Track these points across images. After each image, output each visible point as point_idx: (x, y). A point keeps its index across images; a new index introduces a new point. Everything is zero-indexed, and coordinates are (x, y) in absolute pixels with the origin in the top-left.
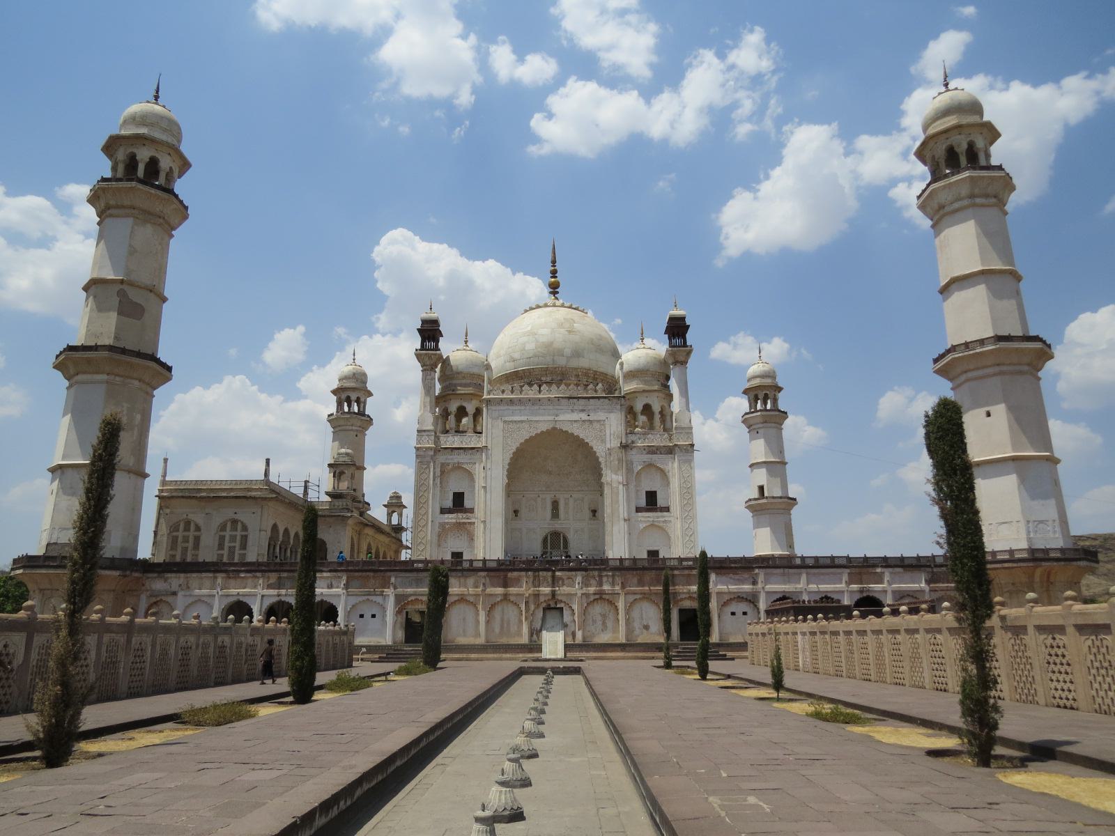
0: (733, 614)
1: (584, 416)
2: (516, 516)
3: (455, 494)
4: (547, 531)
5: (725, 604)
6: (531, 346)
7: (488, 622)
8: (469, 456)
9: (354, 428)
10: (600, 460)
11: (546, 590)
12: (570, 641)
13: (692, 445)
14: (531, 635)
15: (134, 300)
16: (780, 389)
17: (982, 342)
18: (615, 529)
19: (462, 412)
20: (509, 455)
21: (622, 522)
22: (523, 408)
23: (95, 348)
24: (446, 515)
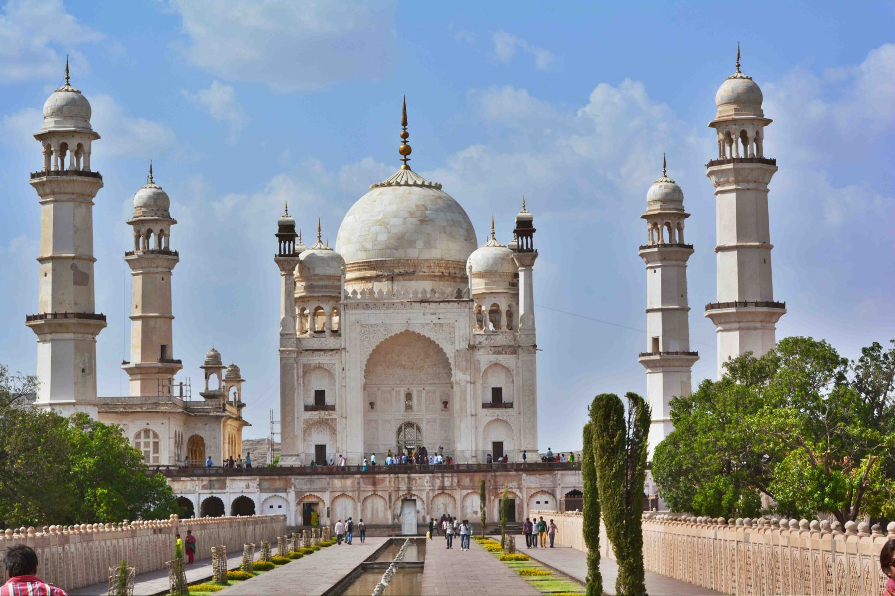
0: (538, 503)
1: (434, 318)
2: (372, 408)
3: (316, 391)
4: (401, 422)
5: (532, 496)
6: (383, 237)
7: (363, 510)
8: (328, 358)
9: (160, 270)
10: (451, 361)
11: (403, 487)
12: (421, 521)
13: (535, 346)
14: (394, 519)
15: (82, 270)
16: (687, 216)
17: (728, 305)
18: (463, 425)
19: (320, 308)
20: (365, 358)
21: (469, 417)
22: (378, 311)
23: (66, 315)
24: (309, 413)
